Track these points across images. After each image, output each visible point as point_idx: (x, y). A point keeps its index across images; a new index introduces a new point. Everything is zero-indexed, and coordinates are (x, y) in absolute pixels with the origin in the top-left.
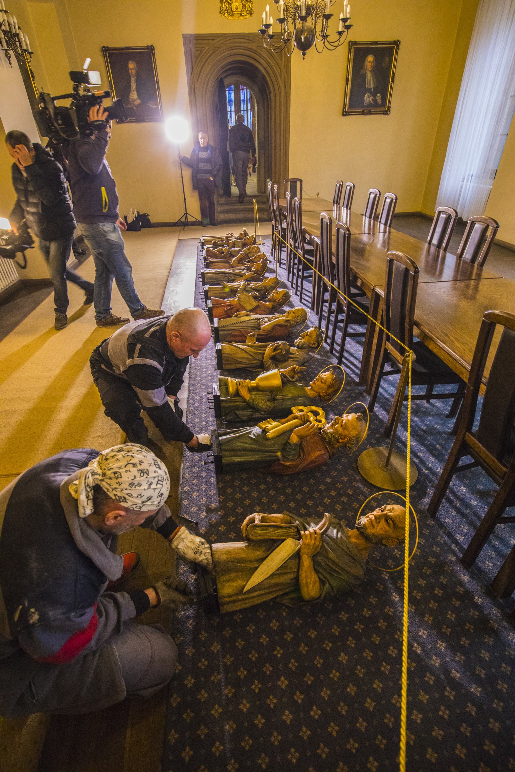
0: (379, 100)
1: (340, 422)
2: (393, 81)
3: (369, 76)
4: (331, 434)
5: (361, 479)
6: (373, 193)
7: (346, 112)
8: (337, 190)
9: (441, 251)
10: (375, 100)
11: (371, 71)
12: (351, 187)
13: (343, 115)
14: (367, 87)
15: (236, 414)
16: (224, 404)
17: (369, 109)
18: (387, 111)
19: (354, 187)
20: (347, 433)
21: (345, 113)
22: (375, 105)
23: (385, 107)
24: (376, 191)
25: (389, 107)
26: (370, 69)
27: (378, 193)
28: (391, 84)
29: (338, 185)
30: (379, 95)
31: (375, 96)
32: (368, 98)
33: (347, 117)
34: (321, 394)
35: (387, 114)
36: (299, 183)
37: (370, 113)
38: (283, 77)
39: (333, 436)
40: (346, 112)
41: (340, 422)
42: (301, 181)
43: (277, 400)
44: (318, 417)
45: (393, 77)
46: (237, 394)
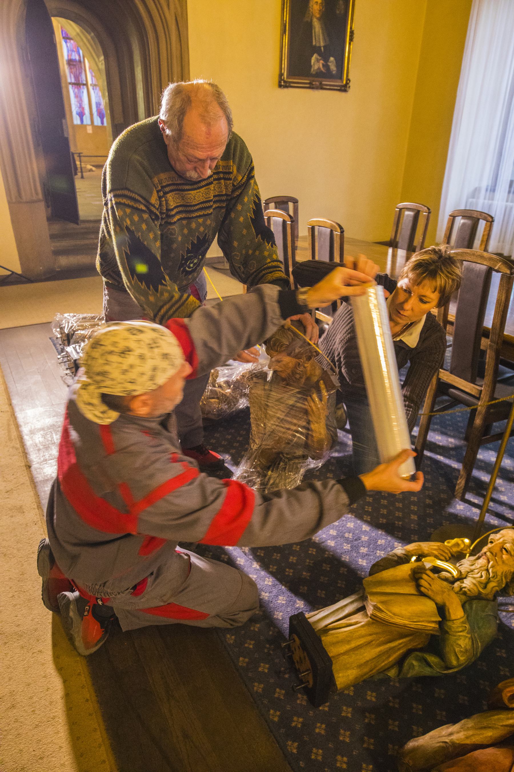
2: (351, 40)
3: (317, 26)
7: (285, 82)
11: (319, 19)
13: (280, 86)
14: (314, 43)
17: (320, 79)
18: (347, 83)
21: (283, 84)
22: (326, 74)
23: (341, 78)
25: (348, 80)
26: (318, 16)
30: (332, 59)
31: (326, 60)
33: (286, 90)
35: (345, 91)
37: (321, 87)
38: (172, 6)
40: (285, 82)
45: (352, 32)
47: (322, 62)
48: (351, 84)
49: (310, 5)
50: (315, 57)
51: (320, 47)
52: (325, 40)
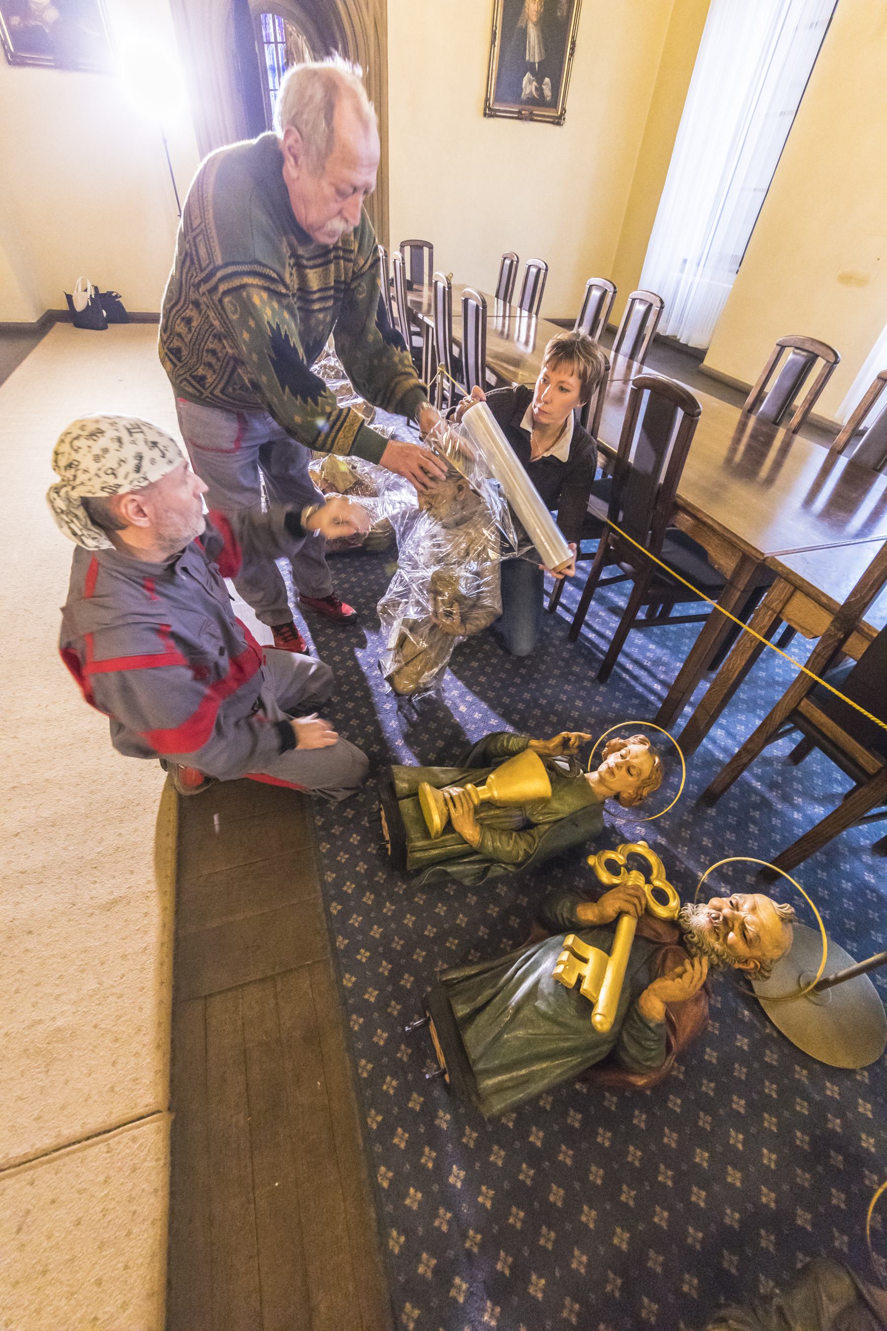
0: (547, 92)
1: (737, 925)
2: (572, 54)
3: (533, 34)
4: (718, 956)
5: (775, 1035)
6: (598, 287)
7: (490, 109)
8: (506, 272)
9: (781, 434)
10: (539, 89)
11: (536, 24)
12: (539, 270)
13: (485, 115)
14: (527, 58)
15: (447, 874)
16: (418, 855)
17: (530, 107)
19: (546, 270)
20: (758, 953)
21: (489, 113)
22: (538, 101)
24: (605, 285)
25: (564, 109)
26: (535, 19)
27: (611, 290)
28: (570, 59)
29: (508, 262)
31: (540, 82)
32: (528, 86)
33: (491, 120)
34: (625, 795)
35: (559, 124)
36: (426, 250)
37: (531, 118)
39: (723, 961)
41: (737, 925)
42: (431, 247)
43: (536, 825)
44: (657, 883)
45: (573, 43)
46: (449, 826)
47: (535, 83)
48: (566, 116)
49: (526, 4)
50: (528, 75)
51: (534, 63)
52: (540, 52)
